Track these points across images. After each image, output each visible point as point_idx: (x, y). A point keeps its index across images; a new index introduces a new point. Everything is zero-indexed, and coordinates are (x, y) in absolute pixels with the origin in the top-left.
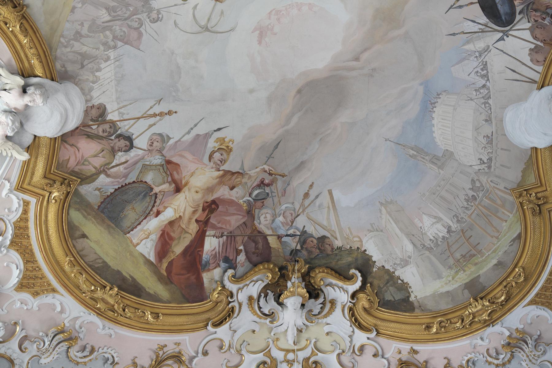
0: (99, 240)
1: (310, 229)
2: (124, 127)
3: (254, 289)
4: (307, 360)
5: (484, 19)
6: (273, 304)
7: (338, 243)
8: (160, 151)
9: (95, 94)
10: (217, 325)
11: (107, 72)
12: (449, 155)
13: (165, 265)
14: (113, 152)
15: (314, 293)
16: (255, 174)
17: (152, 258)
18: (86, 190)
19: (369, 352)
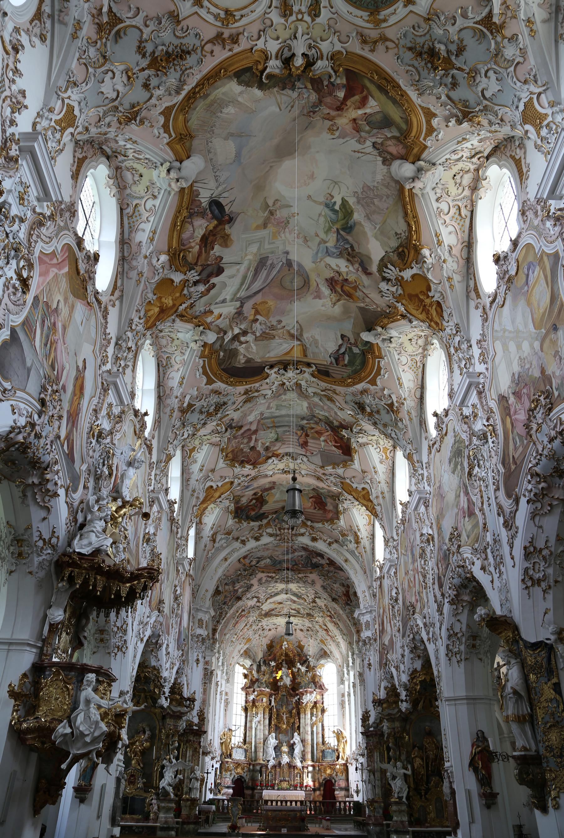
0: (395, 114)
1: (290, 92)
2: (375, 152)
3: (319, 63)
4: (291, 15)
5: (221, 200)
6: (309, 53)
7: (276, 89)
8: (361, 137)
9: (385, 170)
10: (339, 52)
11: (379, 177)
12: (226, 139)
13: (365, 93)
14: (382, 144)
15: (287, 62)
16: (317, 118)
17: (370, 98)
18: (397, 134)
19: (256, 37)
